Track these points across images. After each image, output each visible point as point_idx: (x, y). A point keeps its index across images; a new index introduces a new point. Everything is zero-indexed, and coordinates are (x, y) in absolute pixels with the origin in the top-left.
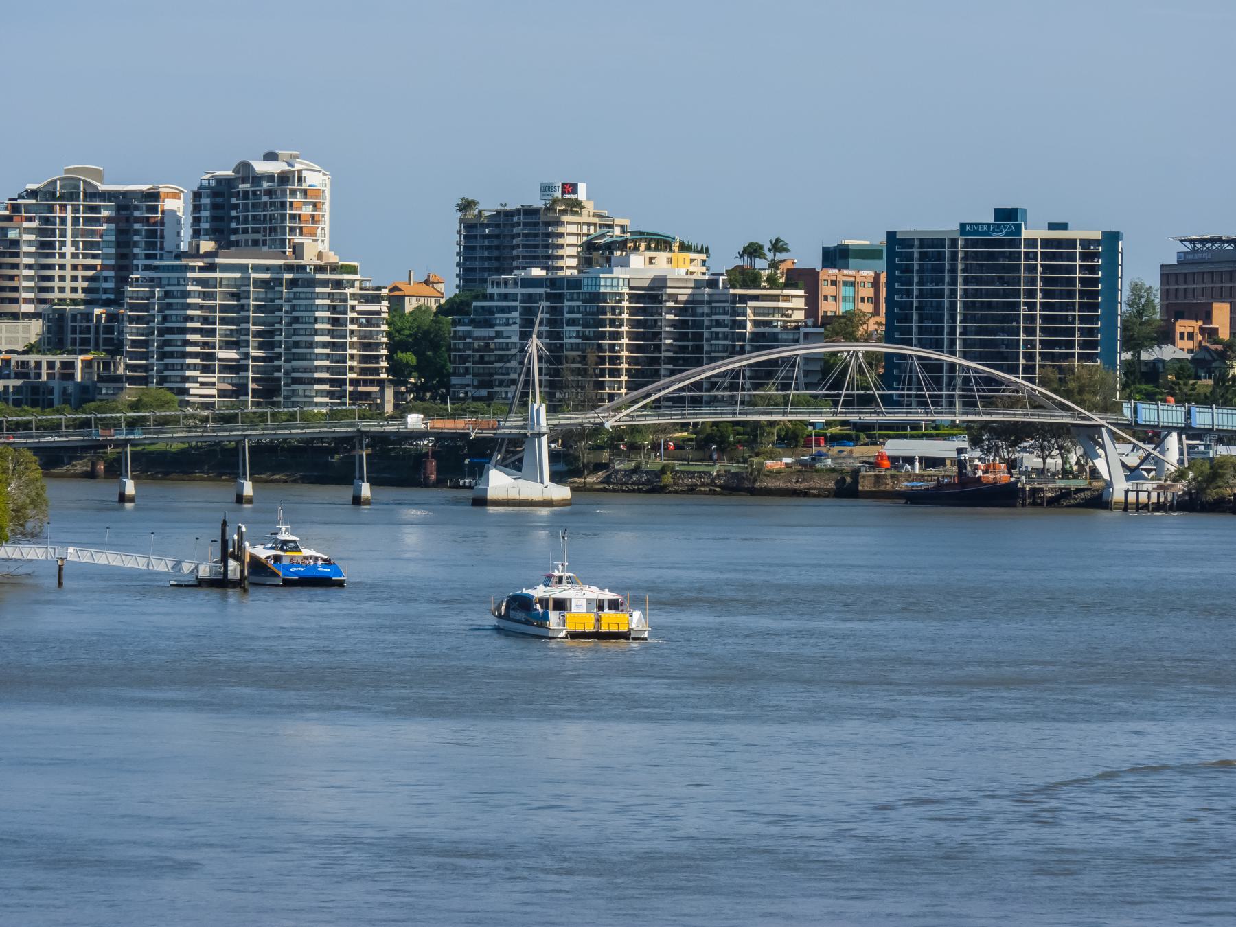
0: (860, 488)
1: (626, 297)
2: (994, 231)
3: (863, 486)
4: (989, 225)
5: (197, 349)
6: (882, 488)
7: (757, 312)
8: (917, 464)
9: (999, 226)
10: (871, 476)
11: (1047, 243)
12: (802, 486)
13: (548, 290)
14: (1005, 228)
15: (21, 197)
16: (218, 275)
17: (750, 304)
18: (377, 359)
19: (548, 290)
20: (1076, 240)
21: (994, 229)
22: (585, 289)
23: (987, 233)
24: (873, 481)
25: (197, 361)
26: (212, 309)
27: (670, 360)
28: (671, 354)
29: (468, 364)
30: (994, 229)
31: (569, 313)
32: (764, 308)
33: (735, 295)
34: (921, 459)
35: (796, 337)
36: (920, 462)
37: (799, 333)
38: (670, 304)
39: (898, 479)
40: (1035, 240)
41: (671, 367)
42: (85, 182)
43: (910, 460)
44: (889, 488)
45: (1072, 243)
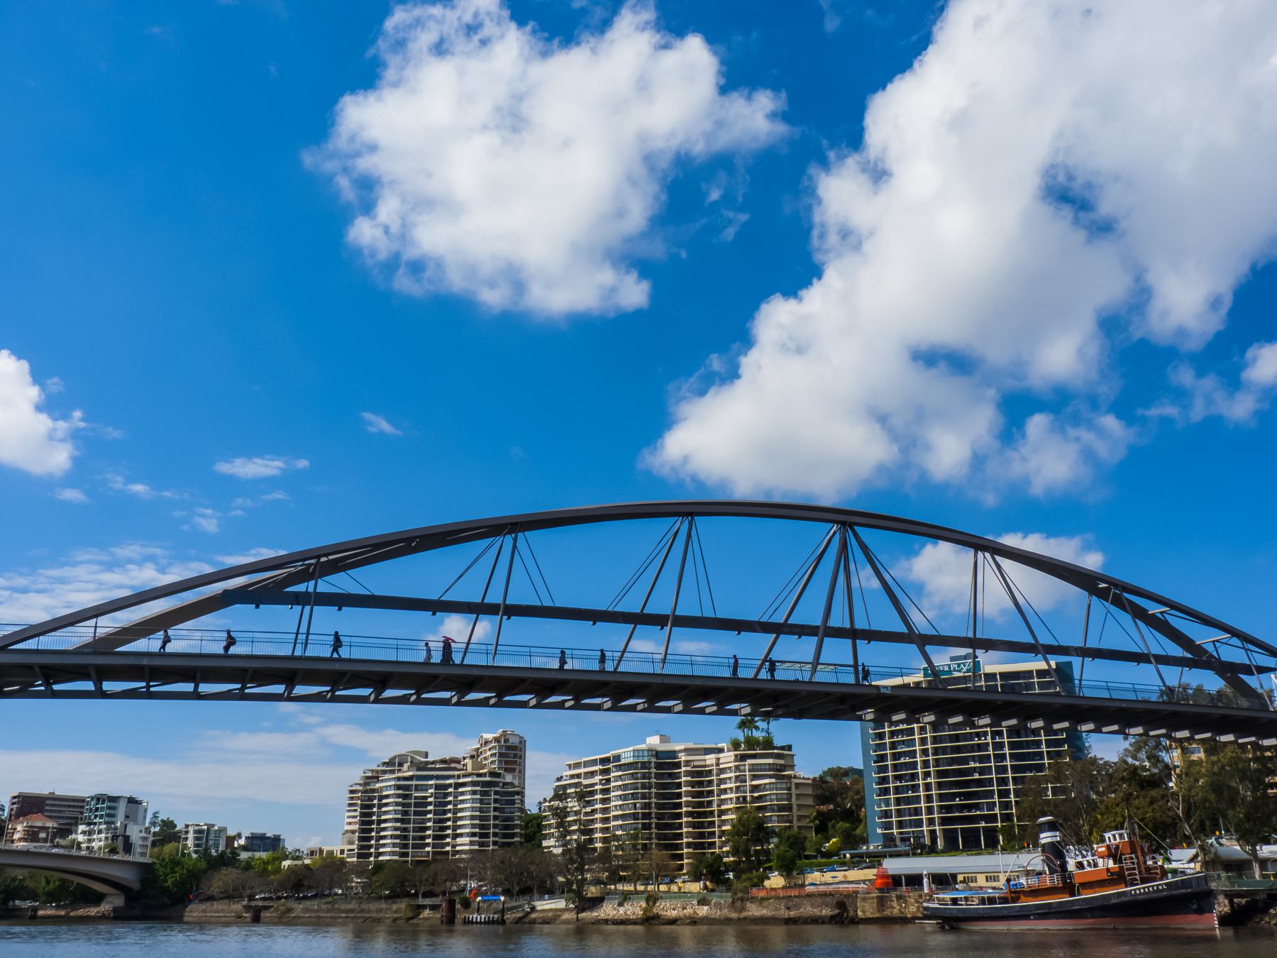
0: (860, 913)
1: (653, 765)
2: (955, 670)
3: (863, 912)
4: (949, 666)
5: (398, 833)
6: (887, 913)
7: (753, 768)
8: (925, 880)
9: (959, 665)
10: (873, 898)
11: (1004, 676)
12: (793, 913)
13: (601, 767)
14: (965, 666)
15: (378, 766)
16: (414, 783)
17: (750, 761)
18: (513, 835)
19: (601, 767)
20: (1032, 671)
21: (954, 668)
22: (623, 761)
23: (950, 672)
24: (875, 905)
25: (398, 841)
26: (409, 805)
27: (689, 814)
28: (690, 809)
29: (552, 831)
30: (954, 668)
31: (615, 781)
32: (761, 764)
33: (736, 756)
34: (929, 874)
35: (789, 785)
36: (929, 878)
37: (791, 783)
38: (689, 768)
39: (906, 902)
40: (995, 675)
41: (690, 819)
42: (412, 757)
43: (914, 880)
44: (896, 911)
45: (1029, 674)
